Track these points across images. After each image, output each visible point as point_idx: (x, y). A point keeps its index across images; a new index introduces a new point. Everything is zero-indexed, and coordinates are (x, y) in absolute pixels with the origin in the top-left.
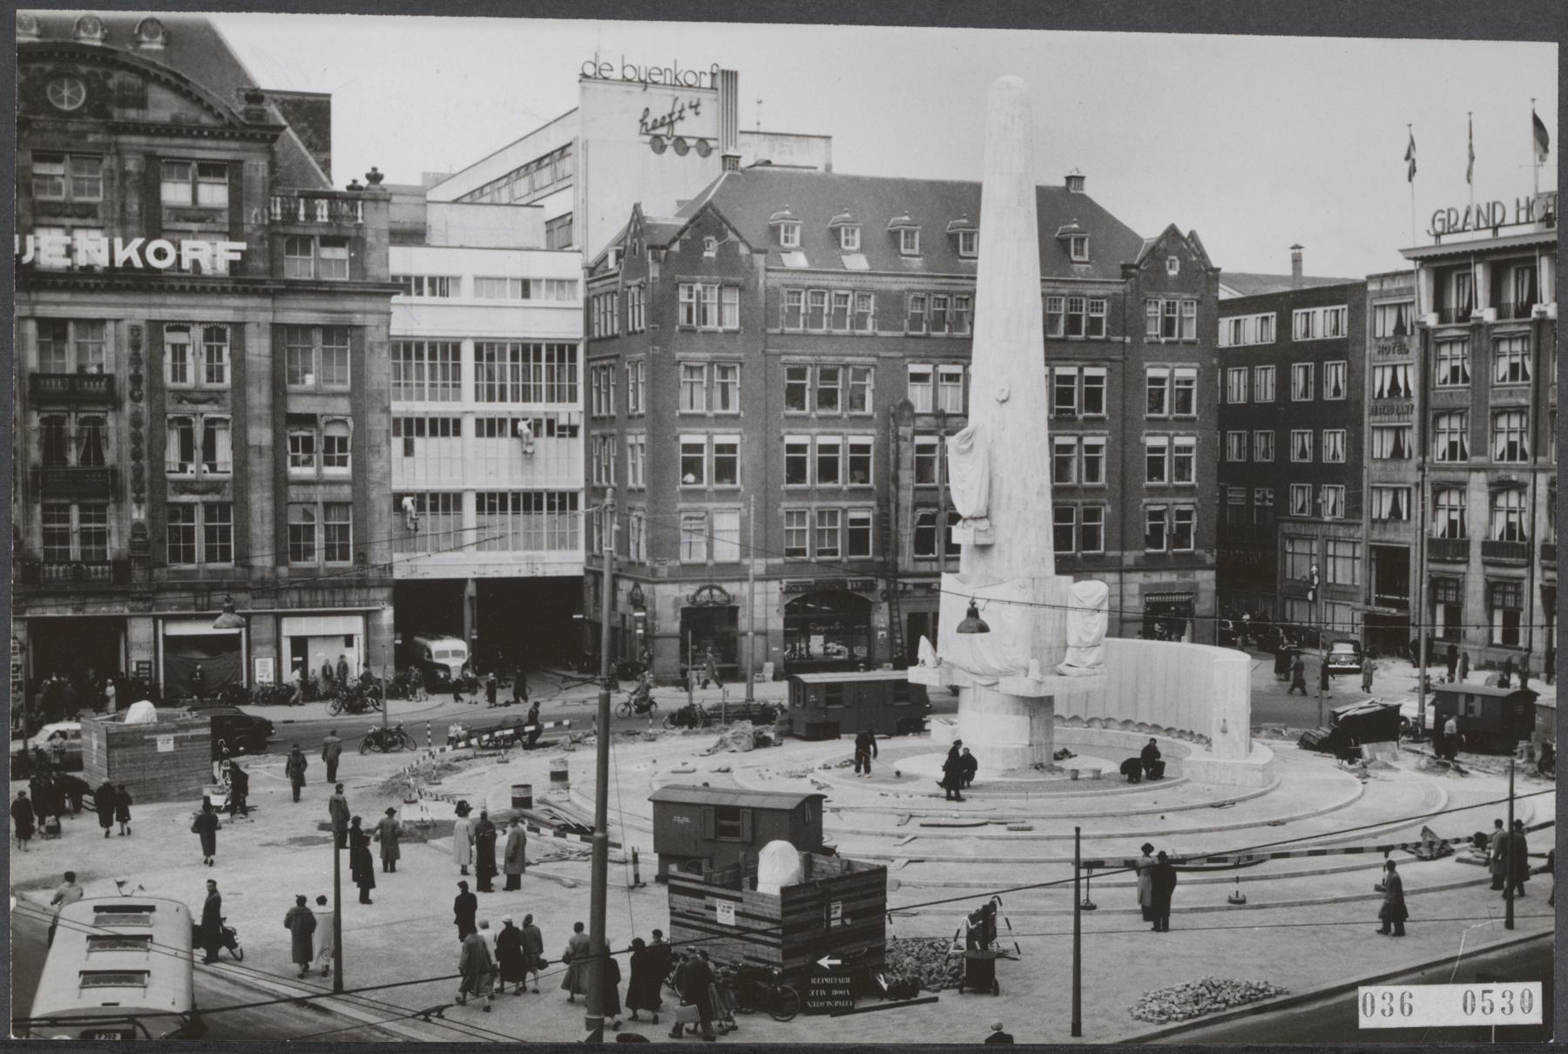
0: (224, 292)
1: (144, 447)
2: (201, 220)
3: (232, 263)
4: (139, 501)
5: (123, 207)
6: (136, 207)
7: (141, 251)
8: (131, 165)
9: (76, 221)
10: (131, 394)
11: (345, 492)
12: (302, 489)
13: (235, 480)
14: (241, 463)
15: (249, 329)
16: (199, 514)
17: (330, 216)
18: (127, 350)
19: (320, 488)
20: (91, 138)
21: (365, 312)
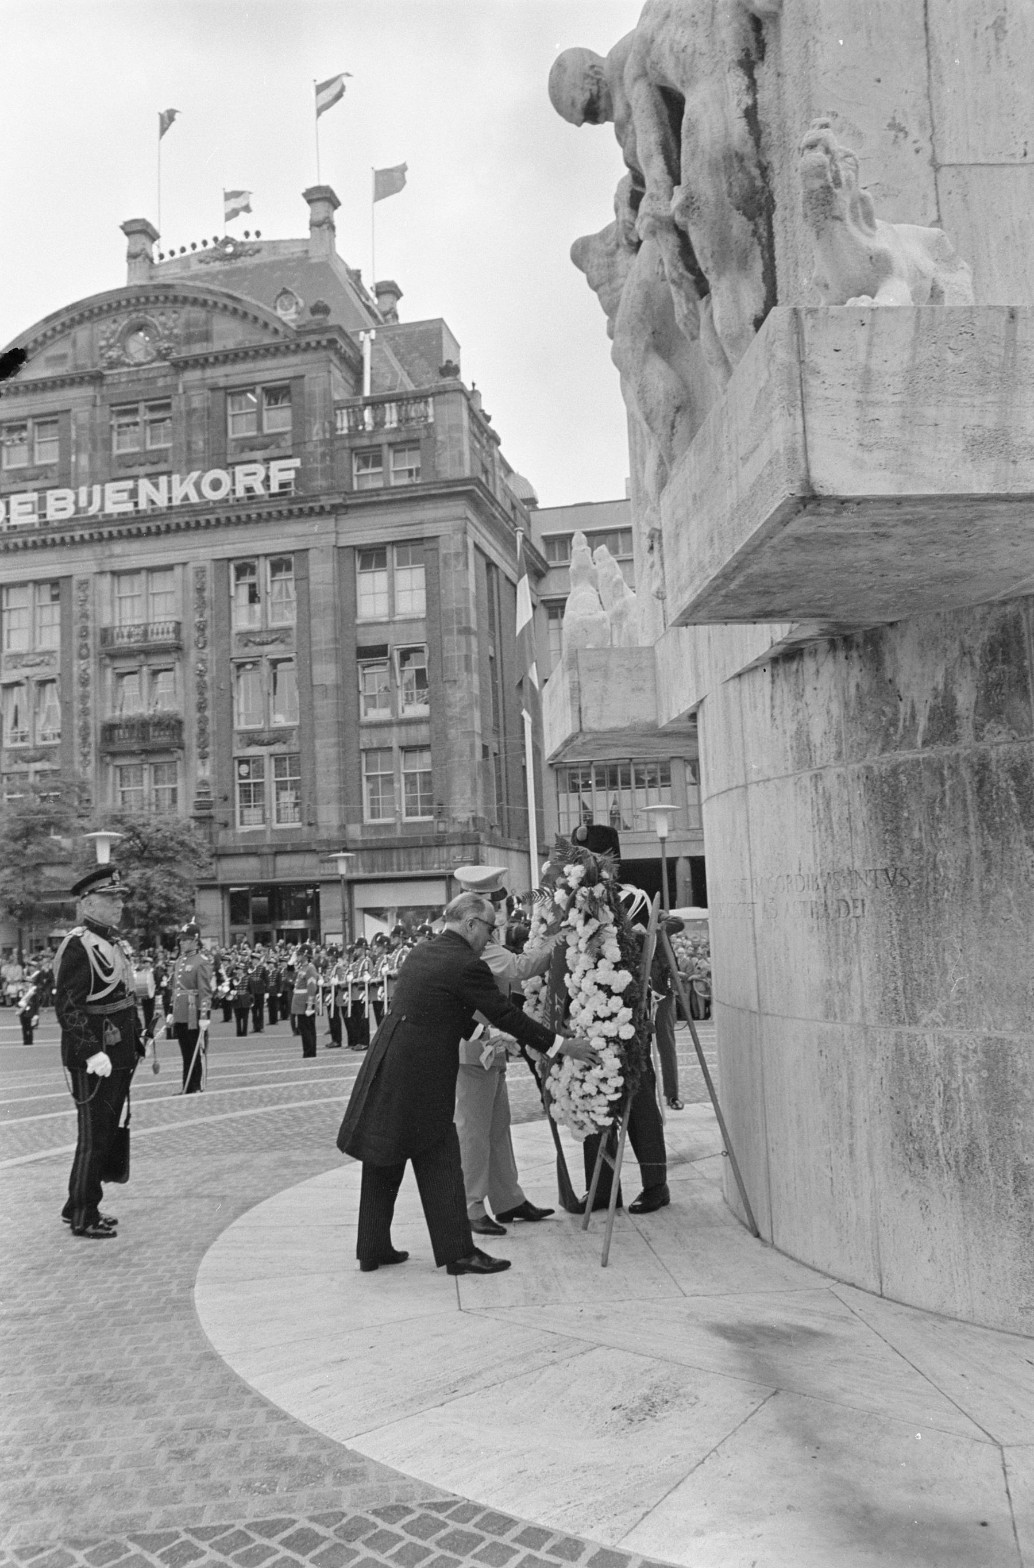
0: (281, 517)
1: (208, 695)
2: (265, 447)
3: (282, 486)
4: (203, 757)
5: (189, 444)
6: (201, 443)
7: (197, 485)
8: (197, 403)
10: (197, 643)
11: (421, 734)
12: (375, 732)
13: (300, 727)
14: (307, 710)
15: (311, 552)
16: (270, 766)
17: (400, 421)
18: (193, 595)
19: (395, 729)
20: (161, 383)
21: (435, 521)
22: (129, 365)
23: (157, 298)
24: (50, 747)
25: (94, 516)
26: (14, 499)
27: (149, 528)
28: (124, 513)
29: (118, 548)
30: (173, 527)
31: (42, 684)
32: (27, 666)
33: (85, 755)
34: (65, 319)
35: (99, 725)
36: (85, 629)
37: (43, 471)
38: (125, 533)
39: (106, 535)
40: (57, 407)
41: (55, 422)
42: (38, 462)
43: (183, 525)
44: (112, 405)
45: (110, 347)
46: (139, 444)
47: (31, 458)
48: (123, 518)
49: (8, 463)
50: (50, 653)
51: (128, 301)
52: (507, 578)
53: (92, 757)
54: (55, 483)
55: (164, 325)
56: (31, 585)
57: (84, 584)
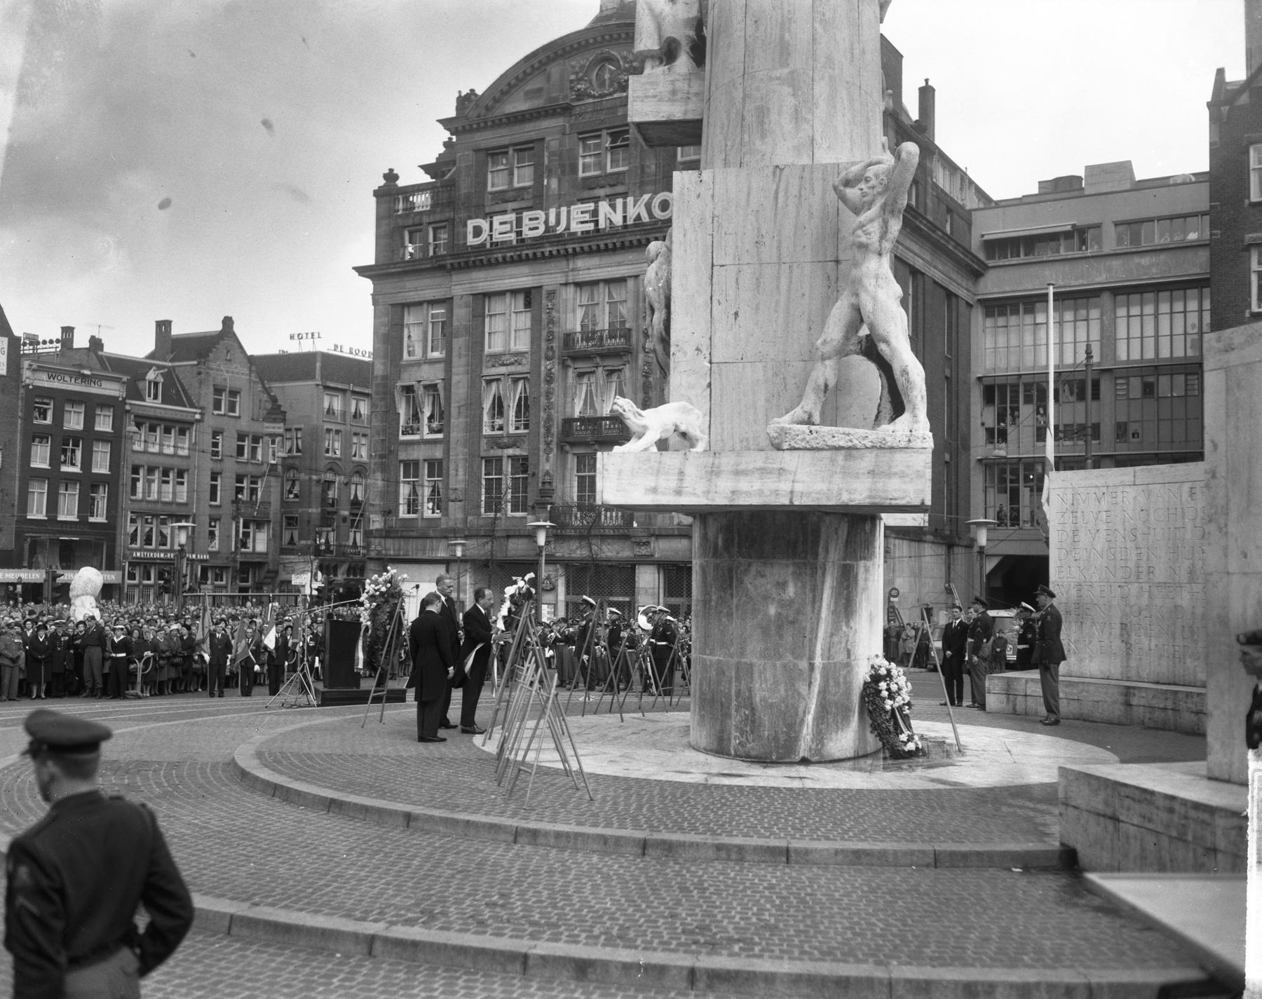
5: (643, 167)
6: (653, 167)
7: (648, 206)
9: (608, 191)
22: (594, 97)
23: (619, 35)
24: (519, 436)
25: (561, 235)
26: (497, 219)
27: (606, 245)
28: (588, 232)
29: (580, 263)
30: (627, 244)
31: (516, 381)
32: (503, 365)
33: (548, 444)
34: (542, 57)
35: (561, 417)
36: (551, 333)
37: (519, 193)
38: (586, 249)
39: (570, 251)
40: (533, 136)
41: (532, 148)
42: (516, 185)
43: (635, 243)
44: (580, 133)
45: (579, 80)
46: (600, 169)
47: (511, 182)
48: (586, 235)
49: (493, 185)
50: (522, 354)
51: (595, 39)
52: (935, 282)
53: (554, 446)
54: (529, 204)
55: (625, 58)
56: (508, 295)
57: (552, 294)
